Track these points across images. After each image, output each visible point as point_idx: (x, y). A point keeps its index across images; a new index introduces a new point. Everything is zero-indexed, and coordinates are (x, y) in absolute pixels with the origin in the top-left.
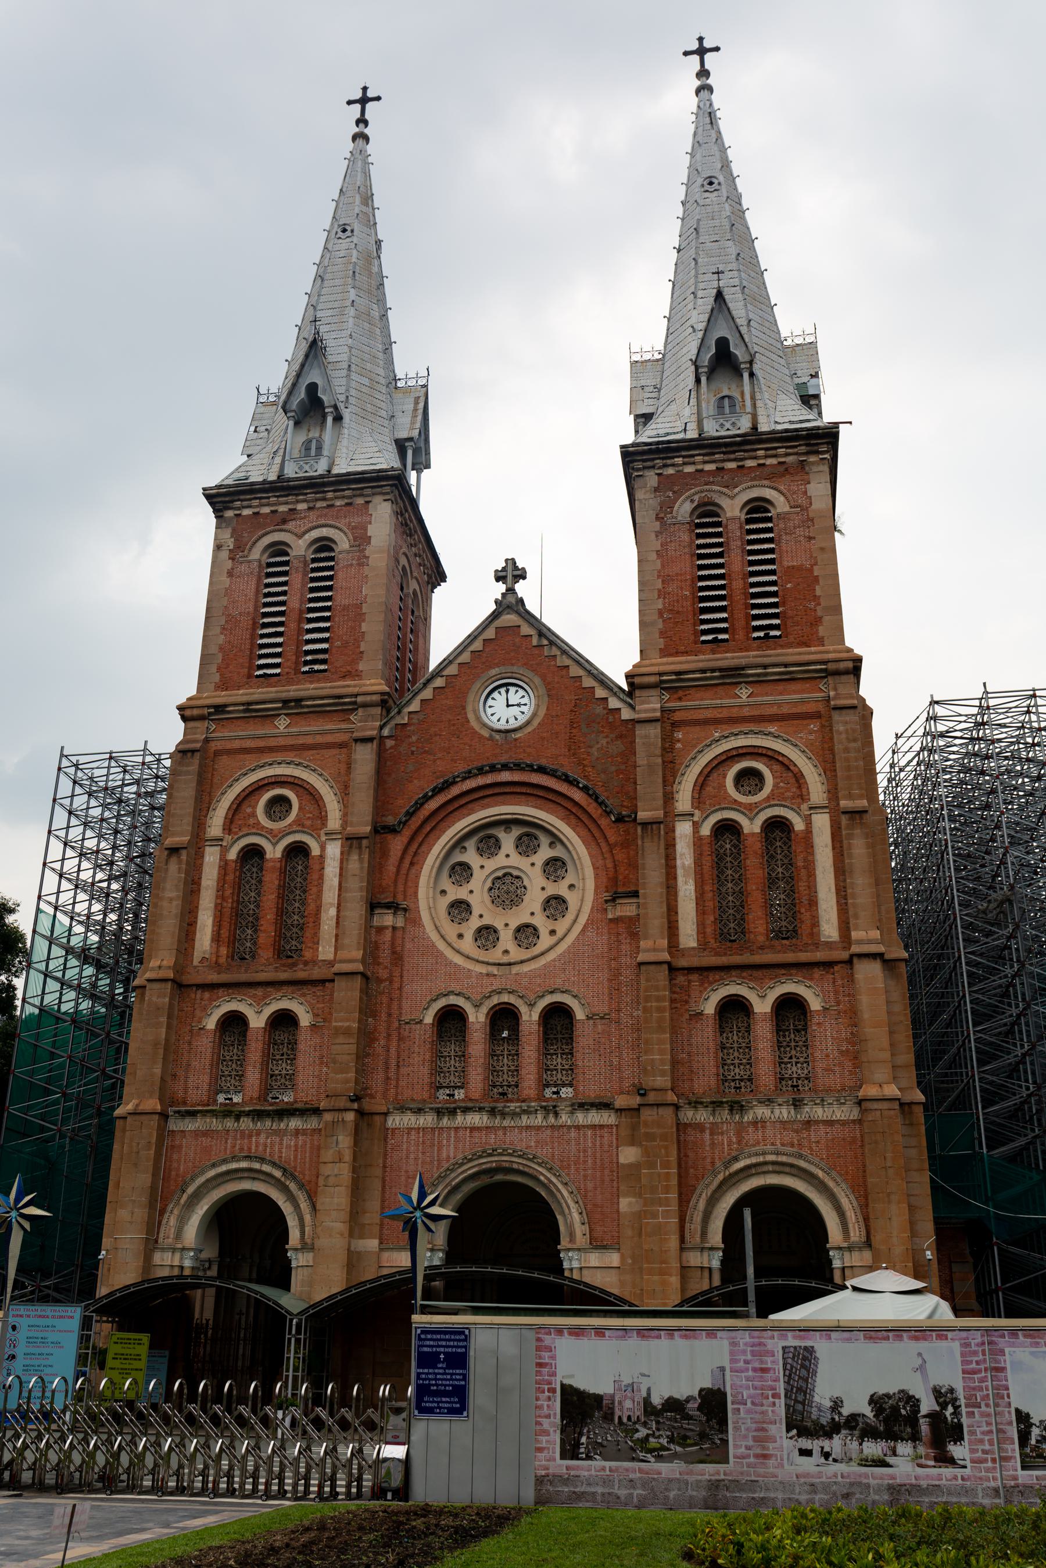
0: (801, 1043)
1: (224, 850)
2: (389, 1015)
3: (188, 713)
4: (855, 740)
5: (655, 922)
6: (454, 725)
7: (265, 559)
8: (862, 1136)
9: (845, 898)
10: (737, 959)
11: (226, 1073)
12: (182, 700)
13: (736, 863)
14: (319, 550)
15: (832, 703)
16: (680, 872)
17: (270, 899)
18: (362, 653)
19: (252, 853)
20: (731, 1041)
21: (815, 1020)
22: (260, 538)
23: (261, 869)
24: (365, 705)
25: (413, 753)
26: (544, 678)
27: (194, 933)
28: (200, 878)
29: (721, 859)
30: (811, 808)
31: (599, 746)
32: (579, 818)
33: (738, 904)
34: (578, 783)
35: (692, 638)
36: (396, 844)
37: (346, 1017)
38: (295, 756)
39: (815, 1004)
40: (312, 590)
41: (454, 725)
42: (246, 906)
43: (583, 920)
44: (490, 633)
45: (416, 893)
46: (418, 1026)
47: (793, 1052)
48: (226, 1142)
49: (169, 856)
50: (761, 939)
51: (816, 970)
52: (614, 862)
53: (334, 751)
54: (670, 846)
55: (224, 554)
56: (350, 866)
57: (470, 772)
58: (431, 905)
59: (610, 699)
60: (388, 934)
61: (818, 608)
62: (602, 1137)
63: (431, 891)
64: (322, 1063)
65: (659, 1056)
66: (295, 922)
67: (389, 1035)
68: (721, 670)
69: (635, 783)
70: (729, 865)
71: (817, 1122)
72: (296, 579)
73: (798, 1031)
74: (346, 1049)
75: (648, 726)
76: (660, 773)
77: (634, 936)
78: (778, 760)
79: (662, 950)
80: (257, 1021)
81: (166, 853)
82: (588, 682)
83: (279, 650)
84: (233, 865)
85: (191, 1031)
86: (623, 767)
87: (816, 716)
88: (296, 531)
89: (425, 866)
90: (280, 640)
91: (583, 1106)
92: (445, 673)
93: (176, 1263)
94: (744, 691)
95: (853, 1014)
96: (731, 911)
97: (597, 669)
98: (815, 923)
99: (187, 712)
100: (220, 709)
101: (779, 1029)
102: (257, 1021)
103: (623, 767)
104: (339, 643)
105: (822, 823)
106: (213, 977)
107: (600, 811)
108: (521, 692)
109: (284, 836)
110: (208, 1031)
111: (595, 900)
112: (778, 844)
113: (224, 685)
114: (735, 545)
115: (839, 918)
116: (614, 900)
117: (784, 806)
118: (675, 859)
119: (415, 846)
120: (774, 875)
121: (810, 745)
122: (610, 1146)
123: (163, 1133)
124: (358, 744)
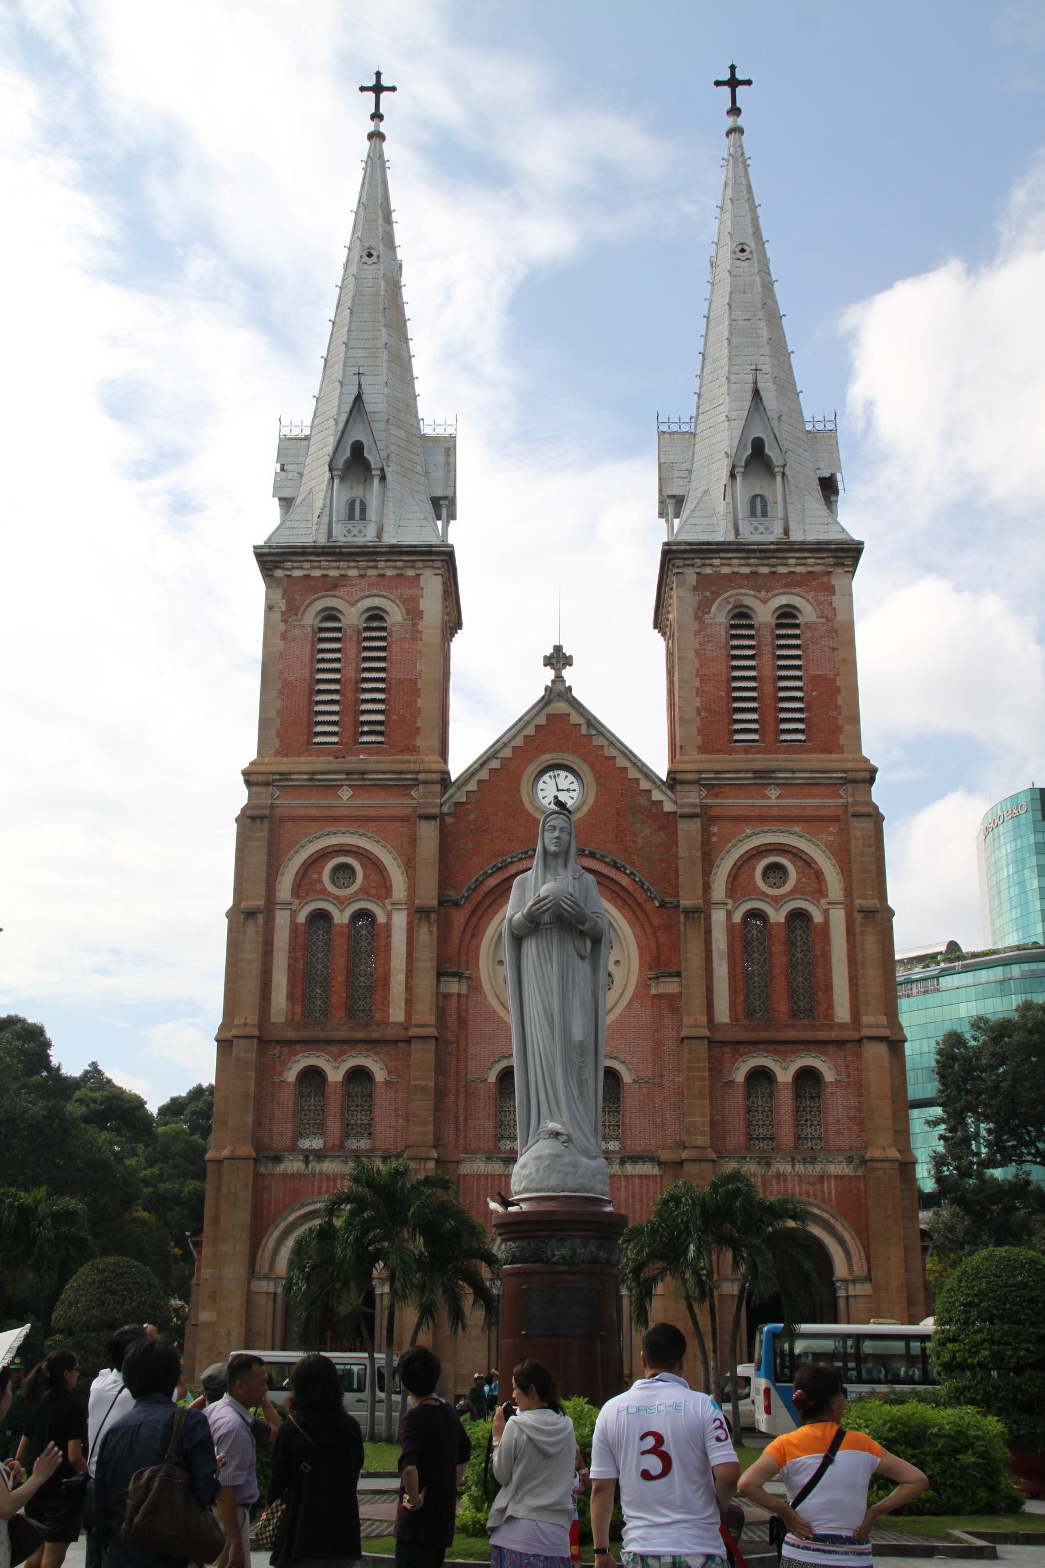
0: (815, 1108)
1: (294, 914)
2: (458, 1074)
3: (253, 778)
4: (870, 846)
5: (697, 1003)
6: (509, 806)
7: (318, 624)
8: (865, 1189)
9: (856, 985)
10: (763, 1035)
11: (305, 1121)
12: (246, 765)
13: (761, 948)
14: (371, 618)
15: (851, 810)
16: (715, 956)
17: (339, 963)
18: (419, 728)
19: (321, 917)
20: (756, 1105)
21: (829, 1090)
22: (313, 602)
23: (328, 932)
24: (425, 782)
25: (471, 830)
26: (592, 766)
27: (270, 992)
28: (272, 940)
29: (749, 943)
30: (829, 903)
31: (643, 835)
32: (625, 901)
33: (762, 984)
34: (625, 869)
35: (726, 738)
36: (459, 917)
37: (423, 1075)
38: (359, 826)
39: (829, 1075)
40: (366, 659)
41: (509, 806)
42: (314, 967)
43: (629, 994)
44: (542, 720)
45: (477, 963)
46: (483, 1084)
47: (808, 1116)
48: (313, 1185)
49: (246, 918)
50: (785, 1017)
51: (830, 1047)
52: (657, 943)
53: (398, 824)
54: (708, 931)
55: (277, 616)
56: (420, 938)
57: (526, 853)
58: (492, 975)
59: (653, 792)
60: (454, 1000)
61: (839, 717)
62: (647, 1185)
63: (491, 961)
64: (397, 1115)
65: (701, 1119)
66: (362, 984)
67: (457, 1092)
68: (755, 772)
69: (677, 872)
70: (755, 949)
71: (829, 1177)
72: (351, 649)
73: (813, 1098)
74: (424, 1105)
75: (689, 821)
76: (700, 866)
77: (675, 1011)
78: (801, 857)
79: (703, 1027)
80: (335, 1075)
81: (242, 916)
82: (633, 774)
83: (336, 718)
84: (303, 928)
85: (273, 1083)
86: (665, 856)
87: (836, 819)
88: (348, 598)
89: (484, 938)
90: (335, 708)
91: (635, 1159)
92: (500, 755)
93: (272, 1290)
94: (773, 792)
95: (858, 1086)
96: (757, 991)
97: (640, 761)
98: (830, 1006)
99: (250, 777)
100: (285, 775)
101: (798, 1095)
102: (335, 1075)
103: (665, 856)
104: (395, 717)
105: (838, 918)
106: (291, 1034)
107: (644, 897)
108: (571, 778)
109: (350, 903)
110: (289, 1083)
111: (640, 976)
112: (798, 932)
113: (284, 750)
114: (767, 649)
115: (851, 1002)
116: (657, 978)
117: (805, 900)
118: (711, 943)
119: (475, 919)
120: (794, 959)
121: (829, 846)
122: (655, 1193)
123: (257, 1175)
124: (422, 821)
